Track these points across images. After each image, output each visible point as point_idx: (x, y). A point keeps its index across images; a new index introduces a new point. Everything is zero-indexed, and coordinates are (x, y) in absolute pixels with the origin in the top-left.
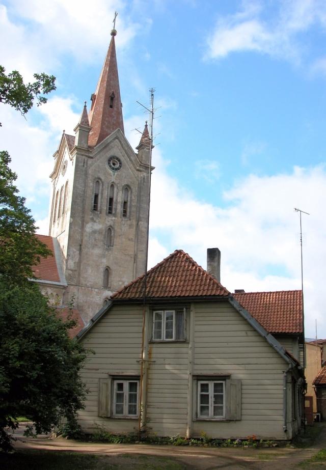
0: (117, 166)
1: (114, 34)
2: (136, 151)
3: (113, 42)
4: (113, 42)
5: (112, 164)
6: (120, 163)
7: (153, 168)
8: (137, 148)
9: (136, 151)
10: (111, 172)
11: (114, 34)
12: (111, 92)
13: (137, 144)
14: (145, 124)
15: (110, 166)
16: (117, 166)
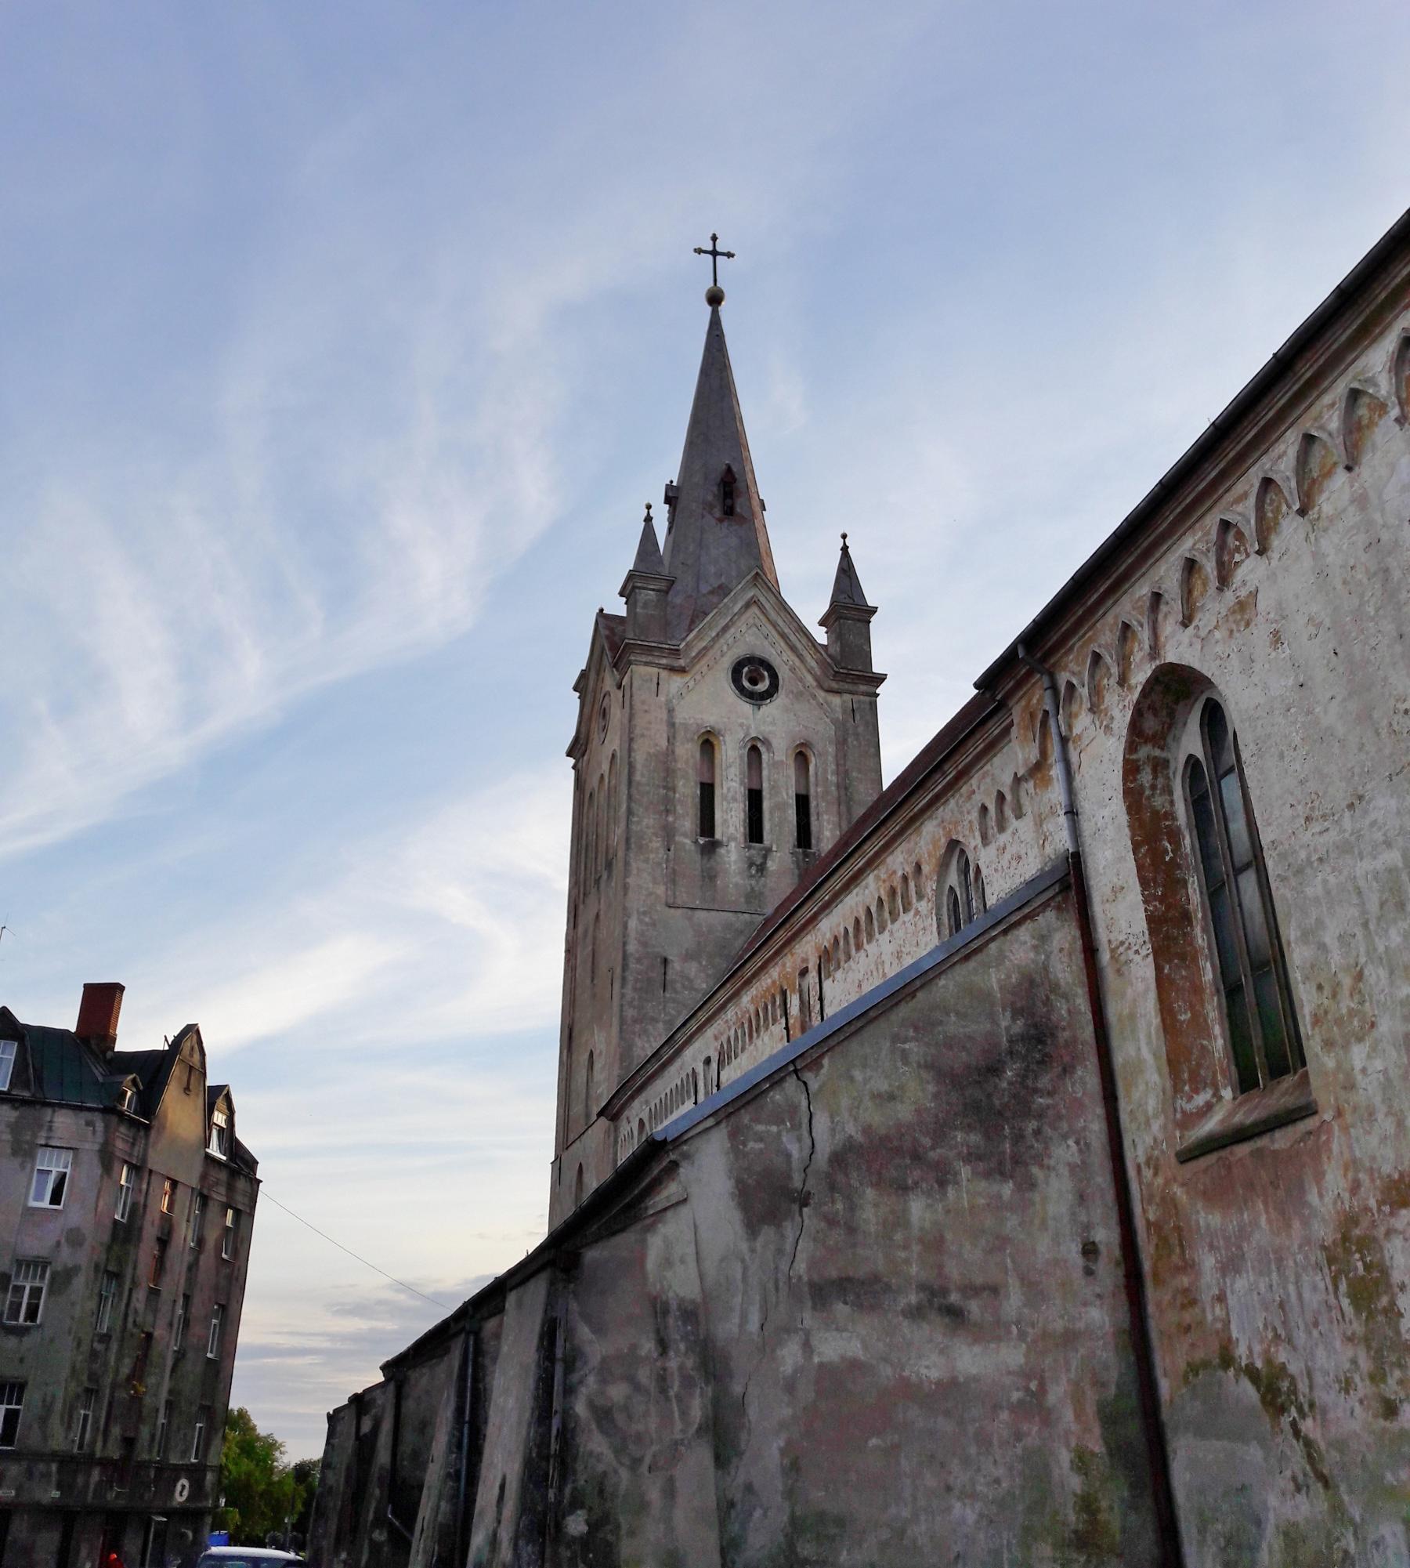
0: (763, 686)
1: (715, 299)
2: (821, 636)
3: (715, 325)
4: (715, 325)
5: (746, 684)
6: (774, 677)
7: (881, 679)
8: (822, 623)
9: (821, 636)
10: (746, 707)
11: (715, 299)
12: (724, 467)
13: (824, 607)
14: (842, 545)
15: (741, 690)
16: (763, 686)
